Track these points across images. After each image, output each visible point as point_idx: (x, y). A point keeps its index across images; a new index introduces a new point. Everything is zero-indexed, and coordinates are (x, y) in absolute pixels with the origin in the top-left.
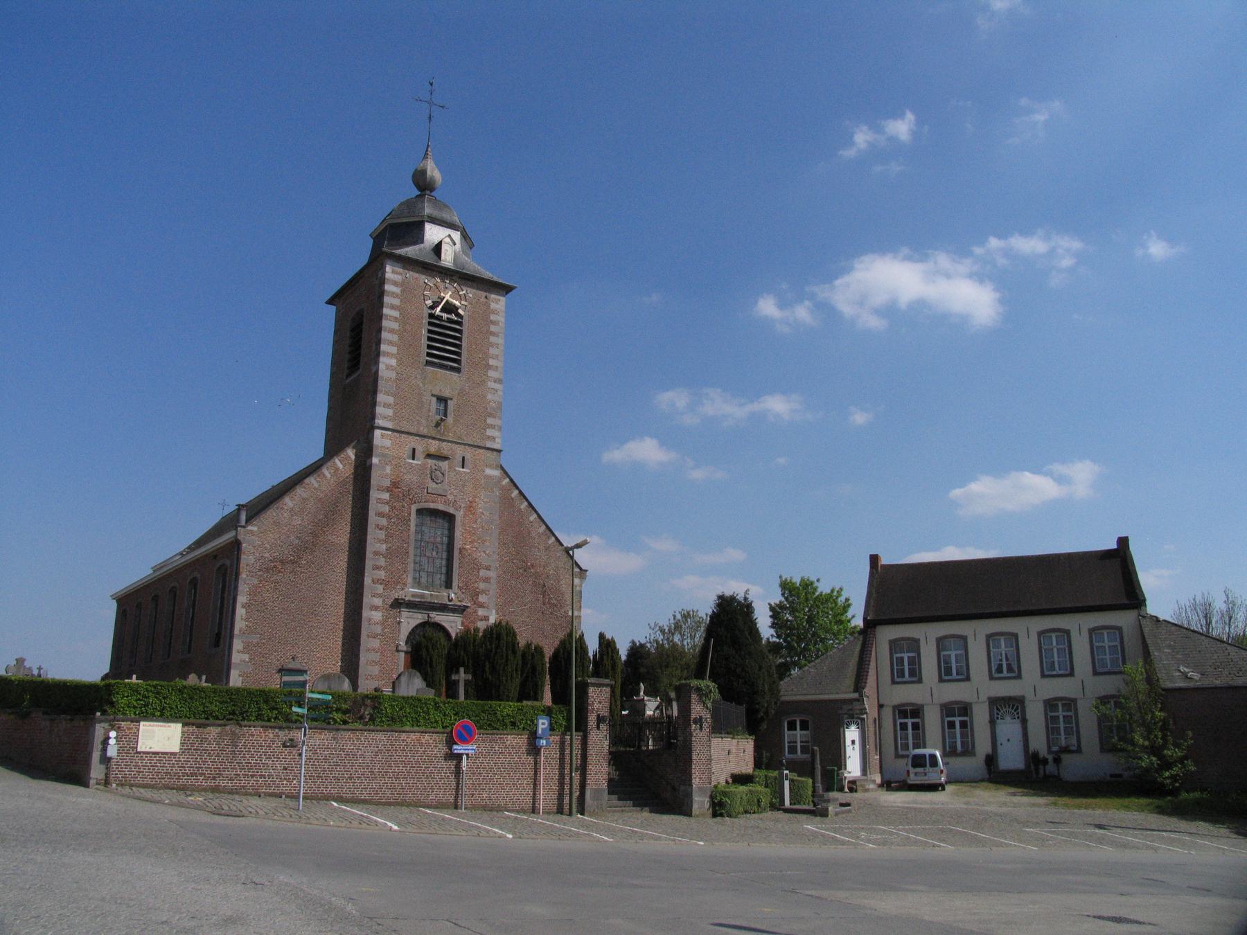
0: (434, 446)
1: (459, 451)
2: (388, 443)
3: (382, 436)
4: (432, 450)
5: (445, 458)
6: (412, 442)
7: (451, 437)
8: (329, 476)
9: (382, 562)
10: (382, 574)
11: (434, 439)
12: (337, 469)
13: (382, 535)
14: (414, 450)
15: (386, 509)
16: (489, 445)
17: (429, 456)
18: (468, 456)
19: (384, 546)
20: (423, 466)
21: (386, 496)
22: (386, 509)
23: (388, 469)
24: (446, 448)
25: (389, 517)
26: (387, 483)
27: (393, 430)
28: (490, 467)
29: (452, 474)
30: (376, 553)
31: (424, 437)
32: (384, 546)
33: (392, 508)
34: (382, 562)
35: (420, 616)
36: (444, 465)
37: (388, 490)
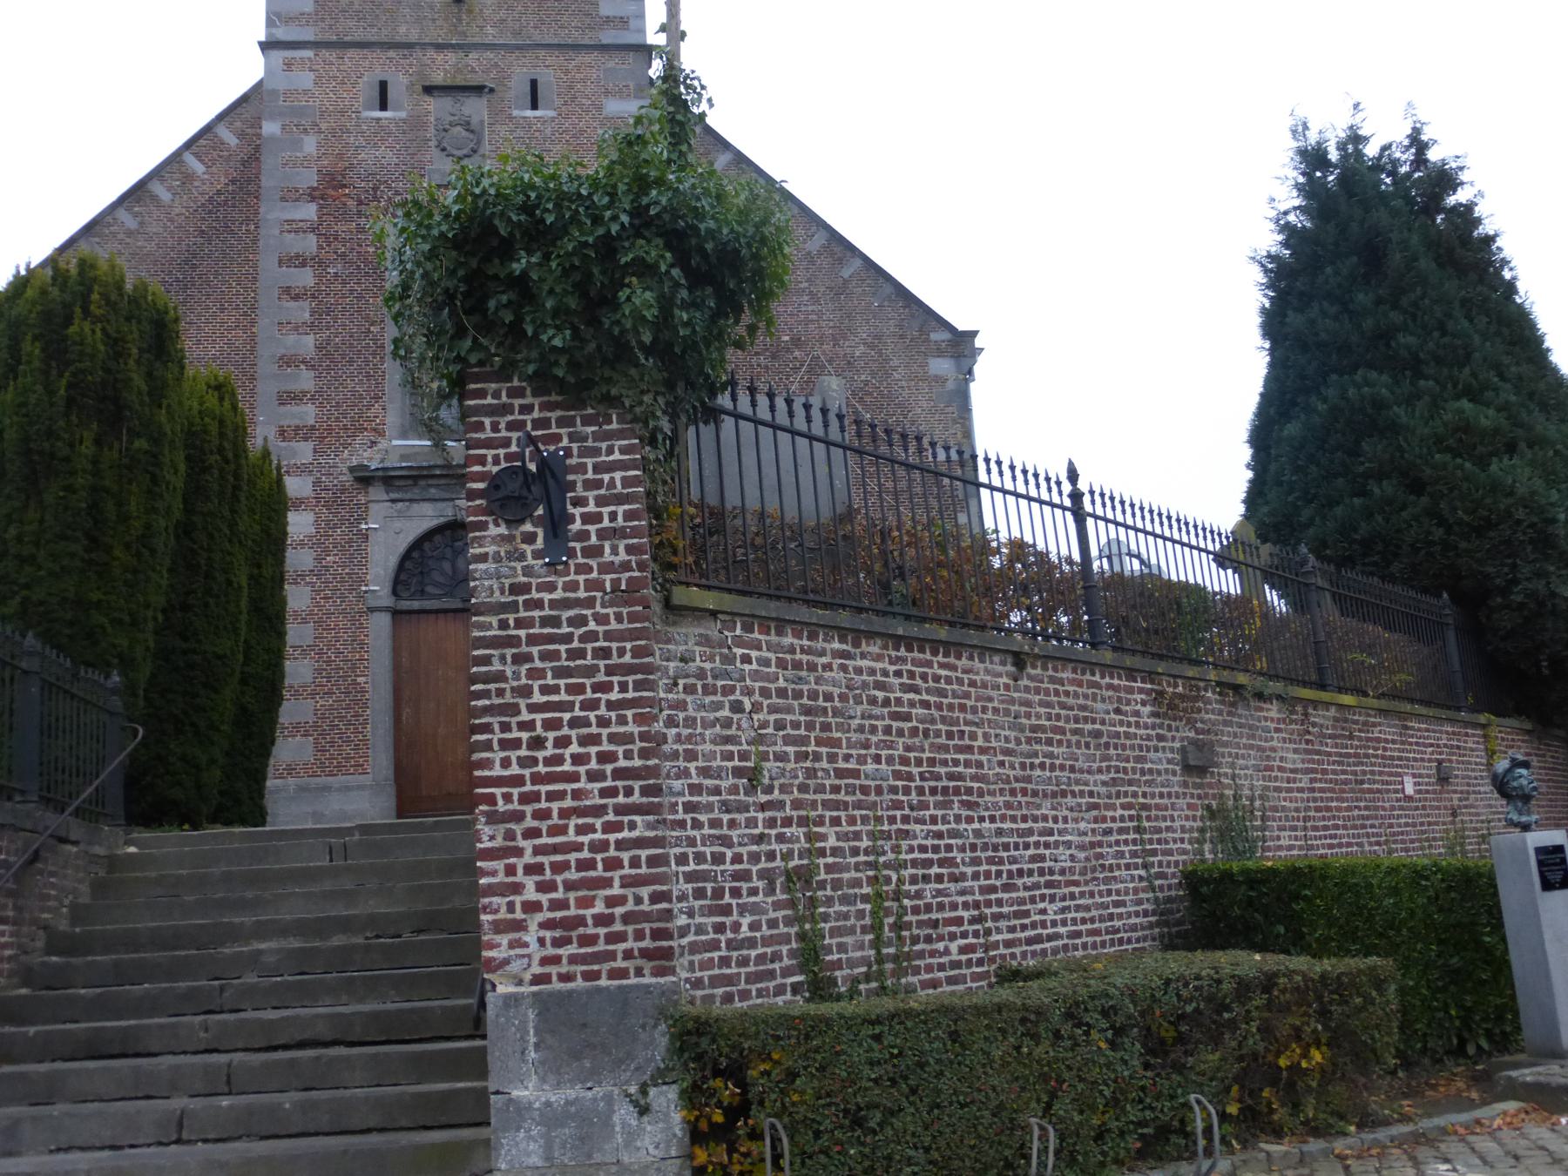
0: (442, 68)
1: (519, 72)
2: (305, 80)
3: (288, 65)
4: (438, 78)
5: (478, 90)
6: (375, 67)
7: (491, 34)
8: (165, 195)
9: (306, 380)
10: (308, 413)
11: (439, 47)
12: (188, 177)
13: (302, 311)
14: (383, 86)
15: (310, 244)
16: (608, 37)
17: (429, 90)
18: (547, 77)
19: (308, 343)
20: (415, 123)
21: (310, 211)
22: (310, 244)
23: (310, 145)
24: (477, 66)
25: (319, 263)
26: (310, 178)
27: (316, 45)
28: (621, 94)
29: (503, 130)
30: (287, 361)
31: (409, 46)
32: (308, 343)
33: (328, 238)
34: (306, 380)
35: (427, 509)
36: (476, 108)
37: (312, 195)
